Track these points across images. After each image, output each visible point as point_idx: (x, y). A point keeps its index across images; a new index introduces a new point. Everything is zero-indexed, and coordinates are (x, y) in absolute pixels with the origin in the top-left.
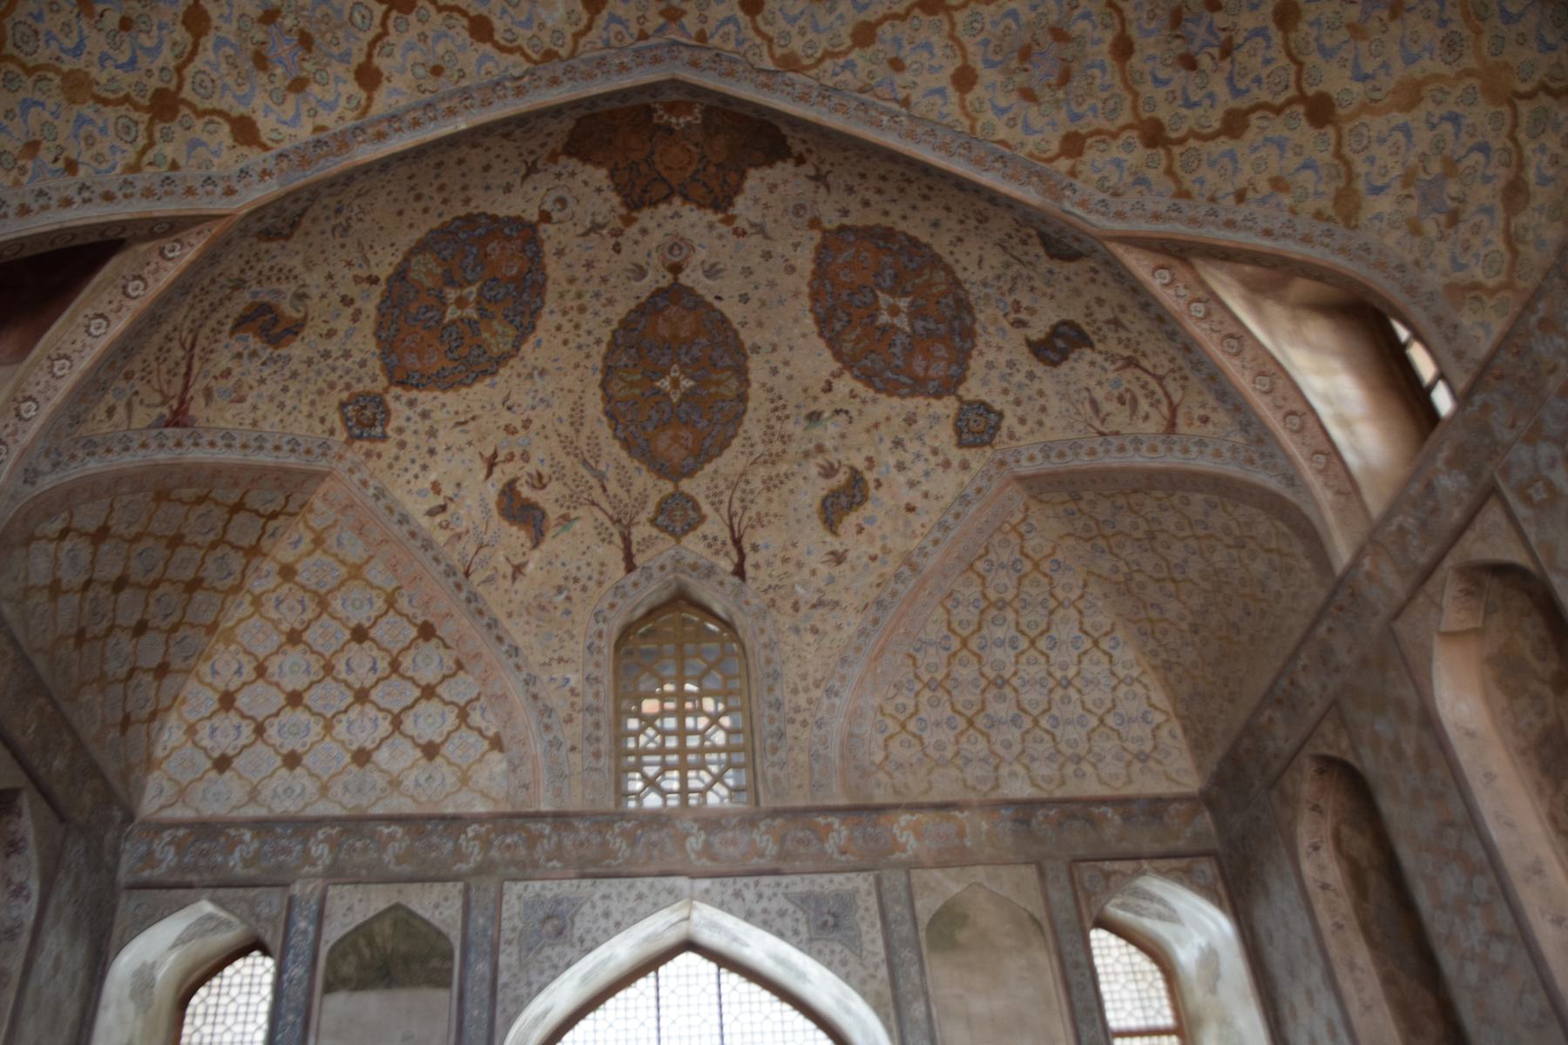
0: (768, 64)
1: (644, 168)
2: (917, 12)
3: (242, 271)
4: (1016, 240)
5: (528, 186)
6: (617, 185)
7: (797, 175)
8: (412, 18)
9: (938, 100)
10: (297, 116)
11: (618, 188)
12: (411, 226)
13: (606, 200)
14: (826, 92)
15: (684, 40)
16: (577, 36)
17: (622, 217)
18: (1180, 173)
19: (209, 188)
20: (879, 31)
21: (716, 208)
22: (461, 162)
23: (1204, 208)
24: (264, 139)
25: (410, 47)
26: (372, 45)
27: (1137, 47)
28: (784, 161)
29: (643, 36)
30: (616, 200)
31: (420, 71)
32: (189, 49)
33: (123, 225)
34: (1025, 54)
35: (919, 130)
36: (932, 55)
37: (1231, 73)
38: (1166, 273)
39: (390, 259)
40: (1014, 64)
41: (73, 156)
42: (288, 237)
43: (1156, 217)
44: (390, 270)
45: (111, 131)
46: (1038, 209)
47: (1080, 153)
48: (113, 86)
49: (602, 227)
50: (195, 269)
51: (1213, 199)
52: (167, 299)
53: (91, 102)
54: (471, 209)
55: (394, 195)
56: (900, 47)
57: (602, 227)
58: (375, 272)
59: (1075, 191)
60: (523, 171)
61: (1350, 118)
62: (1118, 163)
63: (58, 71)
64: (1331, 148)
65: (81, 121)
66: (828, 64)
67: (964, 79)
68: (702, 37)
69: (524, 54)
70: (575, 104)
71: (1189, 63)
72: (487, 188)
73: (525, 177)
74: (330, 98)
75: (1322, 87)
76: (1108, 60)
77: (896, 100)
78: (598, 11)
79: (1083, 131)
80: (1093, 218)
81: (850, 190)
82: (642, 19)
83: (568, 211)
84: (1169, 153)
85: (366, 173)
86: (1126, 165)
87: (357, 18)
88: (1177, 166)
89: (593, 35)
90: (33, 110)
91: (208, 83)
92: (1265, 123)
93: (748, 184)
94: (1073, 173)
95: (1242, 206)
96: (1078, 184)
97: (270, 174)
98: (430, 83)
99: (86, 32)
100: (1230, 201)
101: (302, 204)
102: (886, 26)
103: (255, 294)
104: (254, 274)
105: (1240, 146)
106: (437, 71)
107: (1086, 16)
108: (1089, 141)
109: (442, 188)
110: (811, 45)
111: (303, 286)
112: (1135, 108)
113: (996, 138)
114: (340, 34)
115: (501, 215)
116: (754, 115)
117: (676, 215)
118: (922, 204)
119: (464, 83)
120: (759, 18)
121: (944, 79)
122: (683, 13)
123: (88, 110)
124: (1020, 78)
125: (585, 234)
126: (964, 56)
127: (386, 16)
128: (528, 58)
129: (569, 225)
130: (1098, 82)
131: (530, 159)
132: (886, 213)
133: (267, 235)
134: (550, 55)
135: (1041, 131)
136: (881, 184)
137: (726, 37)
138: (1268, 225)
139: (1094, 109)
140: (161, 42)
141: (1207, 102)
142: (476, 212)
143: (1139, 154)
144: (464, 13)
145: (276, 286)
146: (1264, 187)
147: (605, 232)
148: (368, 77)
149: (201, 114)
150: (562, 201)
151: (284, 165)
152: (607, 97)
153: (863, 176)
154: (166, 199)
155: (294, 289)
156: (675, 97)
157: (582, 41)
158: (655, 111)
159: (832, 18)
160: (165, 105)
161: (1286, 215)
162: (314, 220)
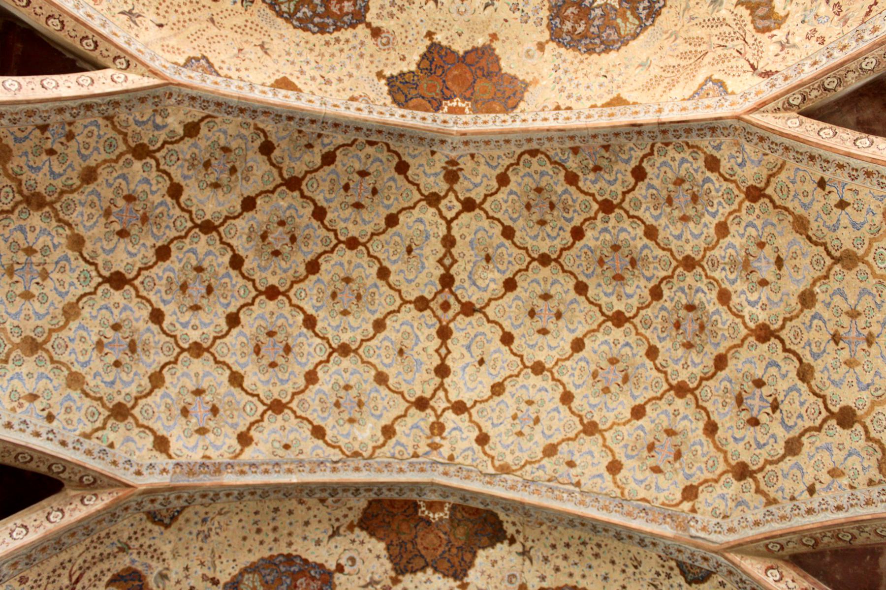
0: (491, 470)
1: (410, 546)
2: (582, 435)
3: (130, 538)
4: (663, 575)
5: (332, 543)
6: (390, 556)
7: (510, 552)
8: (280, 417)
9: (599, 480)
10: (196, 446)
11: (391, 558)
12: (250, 551)
13: (382, 565)
14: (527, 483)
15: (441, 460)
16: (375, 448)
17: (391, 578)
18: (766, 489)
19: (128, 466)
20: (559, 448)
21: (456, 577)
22: (290, 512)
23: (789, 506)
24: (171, 452)
25: (275, 432)
26: (252, 424)
27: (719, 425)
28: (502, 543)
29: (415, 455)
30: (389, 565)
31: (277, 445)
32: (147, 391)
33: (66, 464)
34: (651, 447)
35: (588, 500)
36: (593, 456)
37: (782, 418)
38: (775, 572)
39: (231, 571)
40: (645, 453)
41: (55, 413)
42: (167, 526)
43: (757, 523)
44: (228, 579)
45: (83, 411)
46: (674, 539)
47: (696, 497)
48: (96, 390)
49: (377, 583)
50: (99, 518)
51: (793, 499)
52: (71, 531)
53: (79, 392)
54: (291, 550)
55: (243, 524)
56: (573, 454)
57: (377, 583)
58: (218, 576)
59: (697, 522)
60: (330, 532)
61: (867, 414)
62: (723, 497)
63: (68, 369)
64: (863, 437)
65: (69, 398)
66: (528, 467)
67: (614, 467)
68: (451, 458)
69: (341, 450)
70: (369, 487)
71: (754, 422)
72: (305, 538)
73: (331, 537)
74: (218, 443)
75: (843, 404)
76: (703, 438)
77: (571, 484)
78: (390, 438)
79: (695, 484)
80: (713, 537)
81: (546, 560)
82: (416, 446)
83: (355, 567)
84: (755, 480)
85: (228, 495)
86: (728, 496)
87: (248, 408)
88: (762, 486)
89: (385, 449)
90: (44, 380)
91: (150, 412)
92: (814, 439)
93: (478, 561)
94: (693, 510)
95: (815, 496)
96: (698, 516)
97: (167, 472)
98: (281, 452)
99: (94, 357)
100: (806, 494)
101: (182, 503)
102: (564, 444)
103: (133, 561)
104: (137, 546)
105: (801, 459)
106: (287, 447)
107: (685, 417)
108: (700, 488)
109: (275, 529)
110: (518, 458)
111: (167, 569)
112: (726, 460)
113: (639, 497)
114: (235, 413)
115: (310, 560)
116: (481, 507)
117: (428, 581)
118: (595, 563)
119: (301, 457)
120: (486, 448)
121: (602, 469)
122: (441, 446)
123: (76, 394)
124: (651, 462)
125: (365, 586)
126: (613, 455)
127: (265, 412)
128: (343, 453)
129: (355, 577)
130: (700, 452)
131: (336, 524)
132: (571, 575)
133: (153, 517)
134: (356, 454)
135: (669, 488)
136: (565, 551)
137: (467, 457)
138: (839, 503)
139: (700, 469)
140: (133, 381)
141: (772, 441)
142: (294, 553)
143: (736, 485)
144: (310, 422)
145: (149, 562)
146: (826, 478)
147: (379, 587)
148: (245, 439)
149: (139, 425)
150: (352, 560)
151: (178, 470)
152: (390, 486)
153: (554, 547)
154: (97, 460)
155: (160, 569)
156: (434, 497)
157: (378, 451)
158: (420, 507)
159: (531, 444)
160: (120, 412)
161: (849, 490)
162: (187, 520)
